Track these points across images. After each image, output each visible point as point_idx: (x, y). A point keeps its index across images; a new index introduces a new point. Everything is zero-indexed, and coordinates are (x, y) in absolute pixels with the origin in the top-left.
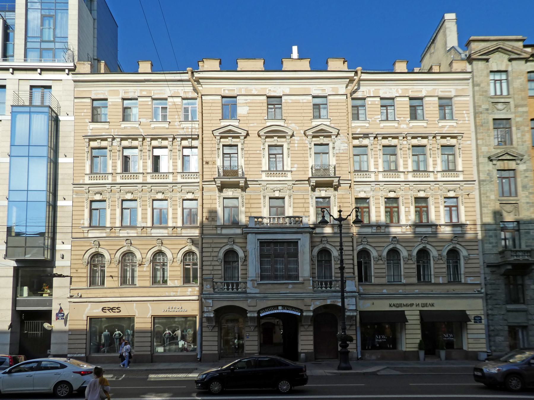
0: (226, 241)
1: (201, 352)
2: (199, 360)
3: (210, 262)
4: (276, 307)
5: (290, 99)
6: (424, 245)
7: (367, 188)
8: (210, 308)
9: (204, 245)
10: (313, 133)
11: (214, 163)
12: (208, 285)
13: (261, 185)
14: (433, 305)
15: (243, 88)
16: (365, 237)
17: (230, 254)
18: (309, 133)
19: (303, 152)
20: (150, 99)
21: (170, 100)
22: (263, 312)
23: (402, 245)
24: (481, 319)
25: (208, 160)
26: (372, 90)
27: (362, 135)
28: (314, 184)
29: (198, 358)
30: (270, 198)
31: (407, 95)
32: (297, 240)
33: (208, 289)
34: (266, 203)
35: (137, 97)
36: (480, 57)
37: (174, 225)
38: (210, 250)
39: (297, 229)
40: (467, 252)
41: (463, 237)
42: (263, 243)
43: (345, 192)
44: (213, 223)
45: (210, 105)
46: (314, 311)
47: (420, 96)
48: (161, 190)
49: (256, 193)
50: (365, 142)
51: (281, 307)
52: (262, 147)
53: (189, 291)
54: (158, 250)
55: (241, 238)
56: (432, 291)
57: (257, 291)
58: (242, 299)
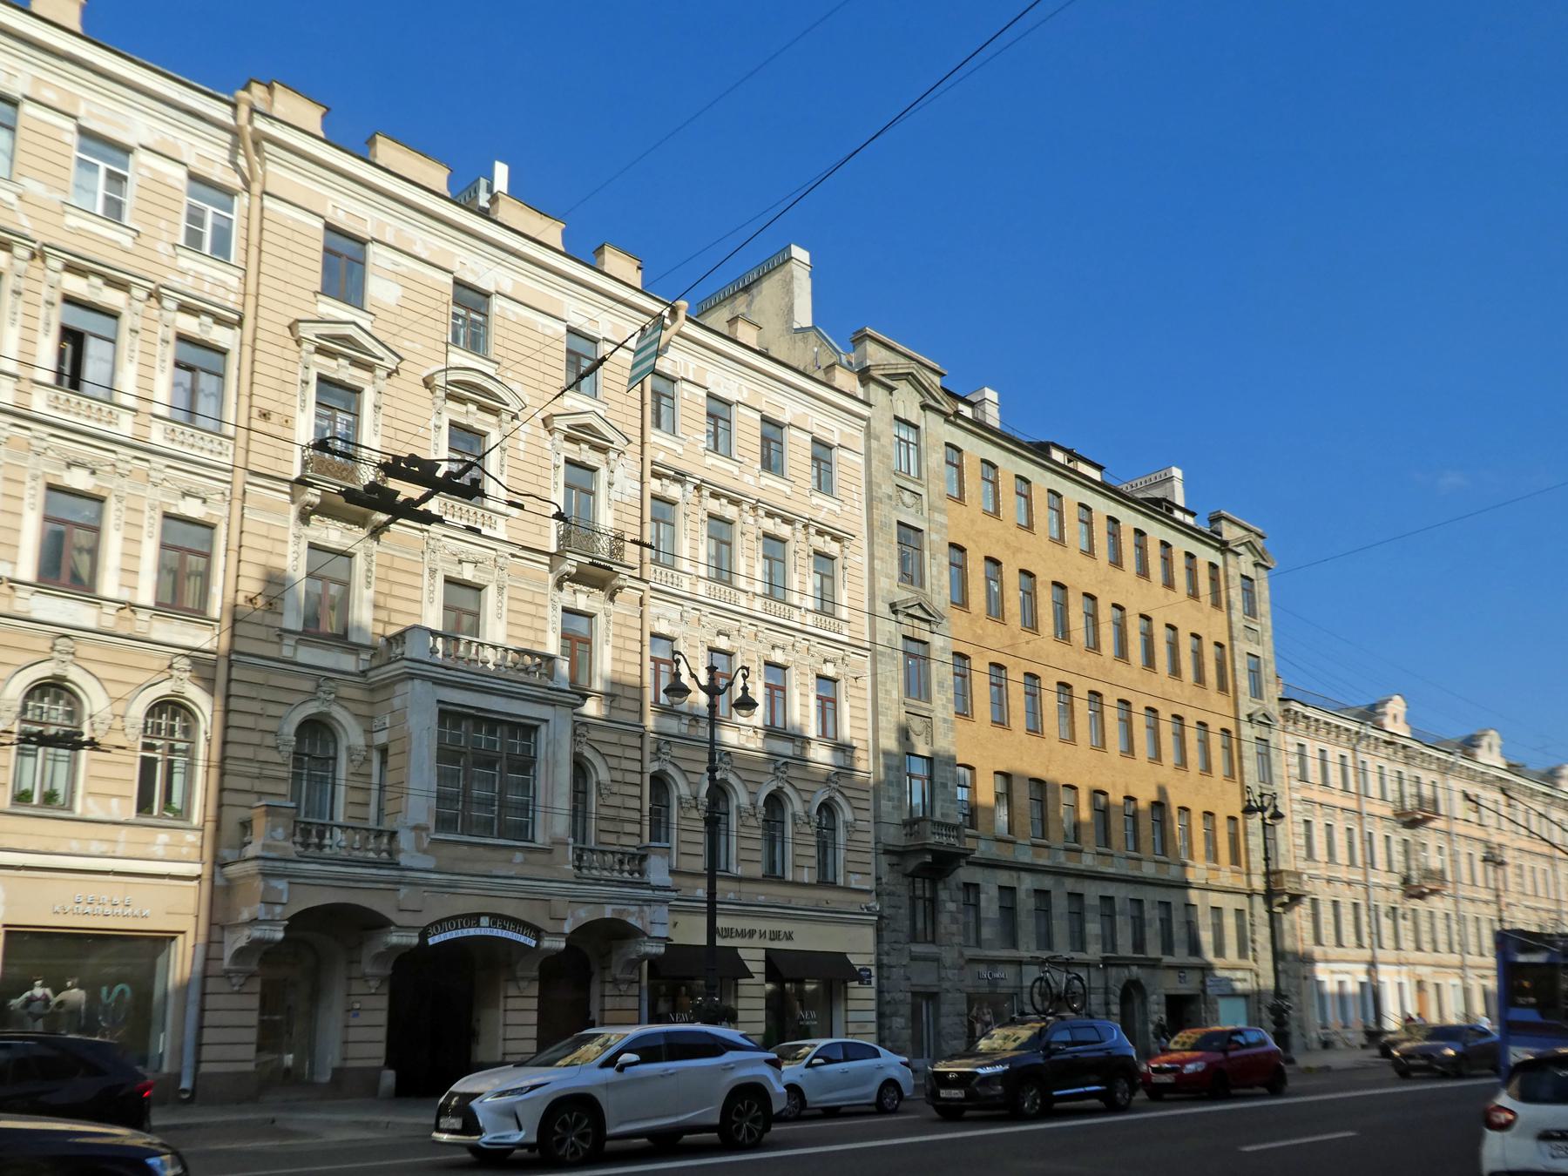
0: (308, 685)
1: (197, 1069)
2: (186, 1096)
3: (251, 749)
4: (473, 918)
5: (513, 312)
6: (780, 785)
7: (673, 612)
8: (278, 909)
9: (235, 688)
10: (569, 427)
11: (287, 421)
12: (280, 830)
13: (426, 533)
14: (789, 937)
15: (390, 225)
16: (668, 742)
17: (317, 729)
18: (561, 424)
19: (537, 470)
20: (70, 125)
21: (142, 157)
22: (437, 930)
23: (739, 777)
24: (870, 976)
25: (267, 405)
26: (691, 366)
27: (673, 473)
28: (574, 570)
29: (184, 1091)
30: (449, 581)
31: (758, 407)
32: (536, 723)
33: (276, 843)
34: (436, 593)
35: (20, 97)
36: (884, 379)
37: (125, 596)
38: (255, 707)
39: (546, 691)
40: (854, 813)
41: (850, 776)
42: (449, 716)
43: (629, 610)
44: (269, 619)
45: (288, 233)
46: (571, 938)
47: (780, 419)
48: (87, 459)
49: (408, 553)
50: (674, 491)
51: (487, 919)
52: (434, 421)
53: (158, 842)
54: (54, 677)
55: (358, 685)
56: (790, 902)
57: (430, 863)
58: (382, 886)
